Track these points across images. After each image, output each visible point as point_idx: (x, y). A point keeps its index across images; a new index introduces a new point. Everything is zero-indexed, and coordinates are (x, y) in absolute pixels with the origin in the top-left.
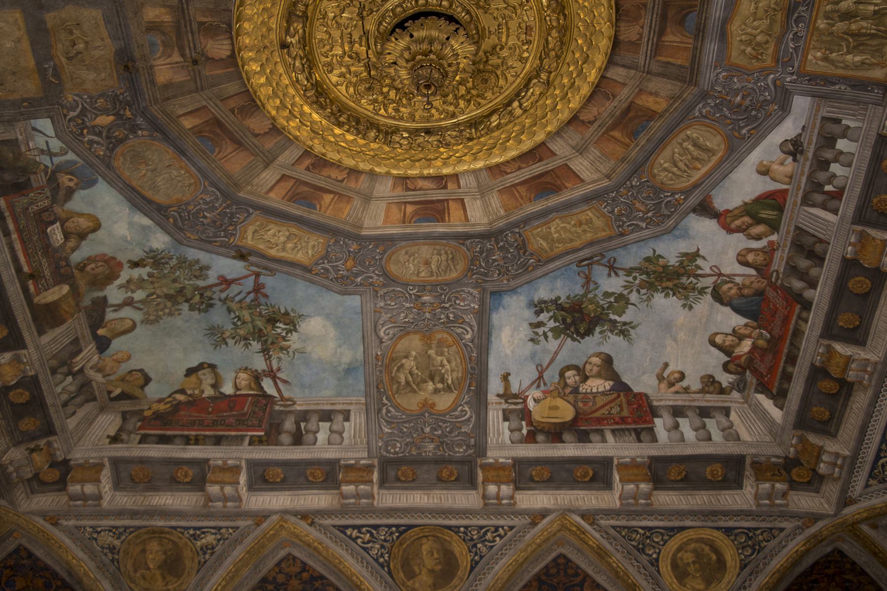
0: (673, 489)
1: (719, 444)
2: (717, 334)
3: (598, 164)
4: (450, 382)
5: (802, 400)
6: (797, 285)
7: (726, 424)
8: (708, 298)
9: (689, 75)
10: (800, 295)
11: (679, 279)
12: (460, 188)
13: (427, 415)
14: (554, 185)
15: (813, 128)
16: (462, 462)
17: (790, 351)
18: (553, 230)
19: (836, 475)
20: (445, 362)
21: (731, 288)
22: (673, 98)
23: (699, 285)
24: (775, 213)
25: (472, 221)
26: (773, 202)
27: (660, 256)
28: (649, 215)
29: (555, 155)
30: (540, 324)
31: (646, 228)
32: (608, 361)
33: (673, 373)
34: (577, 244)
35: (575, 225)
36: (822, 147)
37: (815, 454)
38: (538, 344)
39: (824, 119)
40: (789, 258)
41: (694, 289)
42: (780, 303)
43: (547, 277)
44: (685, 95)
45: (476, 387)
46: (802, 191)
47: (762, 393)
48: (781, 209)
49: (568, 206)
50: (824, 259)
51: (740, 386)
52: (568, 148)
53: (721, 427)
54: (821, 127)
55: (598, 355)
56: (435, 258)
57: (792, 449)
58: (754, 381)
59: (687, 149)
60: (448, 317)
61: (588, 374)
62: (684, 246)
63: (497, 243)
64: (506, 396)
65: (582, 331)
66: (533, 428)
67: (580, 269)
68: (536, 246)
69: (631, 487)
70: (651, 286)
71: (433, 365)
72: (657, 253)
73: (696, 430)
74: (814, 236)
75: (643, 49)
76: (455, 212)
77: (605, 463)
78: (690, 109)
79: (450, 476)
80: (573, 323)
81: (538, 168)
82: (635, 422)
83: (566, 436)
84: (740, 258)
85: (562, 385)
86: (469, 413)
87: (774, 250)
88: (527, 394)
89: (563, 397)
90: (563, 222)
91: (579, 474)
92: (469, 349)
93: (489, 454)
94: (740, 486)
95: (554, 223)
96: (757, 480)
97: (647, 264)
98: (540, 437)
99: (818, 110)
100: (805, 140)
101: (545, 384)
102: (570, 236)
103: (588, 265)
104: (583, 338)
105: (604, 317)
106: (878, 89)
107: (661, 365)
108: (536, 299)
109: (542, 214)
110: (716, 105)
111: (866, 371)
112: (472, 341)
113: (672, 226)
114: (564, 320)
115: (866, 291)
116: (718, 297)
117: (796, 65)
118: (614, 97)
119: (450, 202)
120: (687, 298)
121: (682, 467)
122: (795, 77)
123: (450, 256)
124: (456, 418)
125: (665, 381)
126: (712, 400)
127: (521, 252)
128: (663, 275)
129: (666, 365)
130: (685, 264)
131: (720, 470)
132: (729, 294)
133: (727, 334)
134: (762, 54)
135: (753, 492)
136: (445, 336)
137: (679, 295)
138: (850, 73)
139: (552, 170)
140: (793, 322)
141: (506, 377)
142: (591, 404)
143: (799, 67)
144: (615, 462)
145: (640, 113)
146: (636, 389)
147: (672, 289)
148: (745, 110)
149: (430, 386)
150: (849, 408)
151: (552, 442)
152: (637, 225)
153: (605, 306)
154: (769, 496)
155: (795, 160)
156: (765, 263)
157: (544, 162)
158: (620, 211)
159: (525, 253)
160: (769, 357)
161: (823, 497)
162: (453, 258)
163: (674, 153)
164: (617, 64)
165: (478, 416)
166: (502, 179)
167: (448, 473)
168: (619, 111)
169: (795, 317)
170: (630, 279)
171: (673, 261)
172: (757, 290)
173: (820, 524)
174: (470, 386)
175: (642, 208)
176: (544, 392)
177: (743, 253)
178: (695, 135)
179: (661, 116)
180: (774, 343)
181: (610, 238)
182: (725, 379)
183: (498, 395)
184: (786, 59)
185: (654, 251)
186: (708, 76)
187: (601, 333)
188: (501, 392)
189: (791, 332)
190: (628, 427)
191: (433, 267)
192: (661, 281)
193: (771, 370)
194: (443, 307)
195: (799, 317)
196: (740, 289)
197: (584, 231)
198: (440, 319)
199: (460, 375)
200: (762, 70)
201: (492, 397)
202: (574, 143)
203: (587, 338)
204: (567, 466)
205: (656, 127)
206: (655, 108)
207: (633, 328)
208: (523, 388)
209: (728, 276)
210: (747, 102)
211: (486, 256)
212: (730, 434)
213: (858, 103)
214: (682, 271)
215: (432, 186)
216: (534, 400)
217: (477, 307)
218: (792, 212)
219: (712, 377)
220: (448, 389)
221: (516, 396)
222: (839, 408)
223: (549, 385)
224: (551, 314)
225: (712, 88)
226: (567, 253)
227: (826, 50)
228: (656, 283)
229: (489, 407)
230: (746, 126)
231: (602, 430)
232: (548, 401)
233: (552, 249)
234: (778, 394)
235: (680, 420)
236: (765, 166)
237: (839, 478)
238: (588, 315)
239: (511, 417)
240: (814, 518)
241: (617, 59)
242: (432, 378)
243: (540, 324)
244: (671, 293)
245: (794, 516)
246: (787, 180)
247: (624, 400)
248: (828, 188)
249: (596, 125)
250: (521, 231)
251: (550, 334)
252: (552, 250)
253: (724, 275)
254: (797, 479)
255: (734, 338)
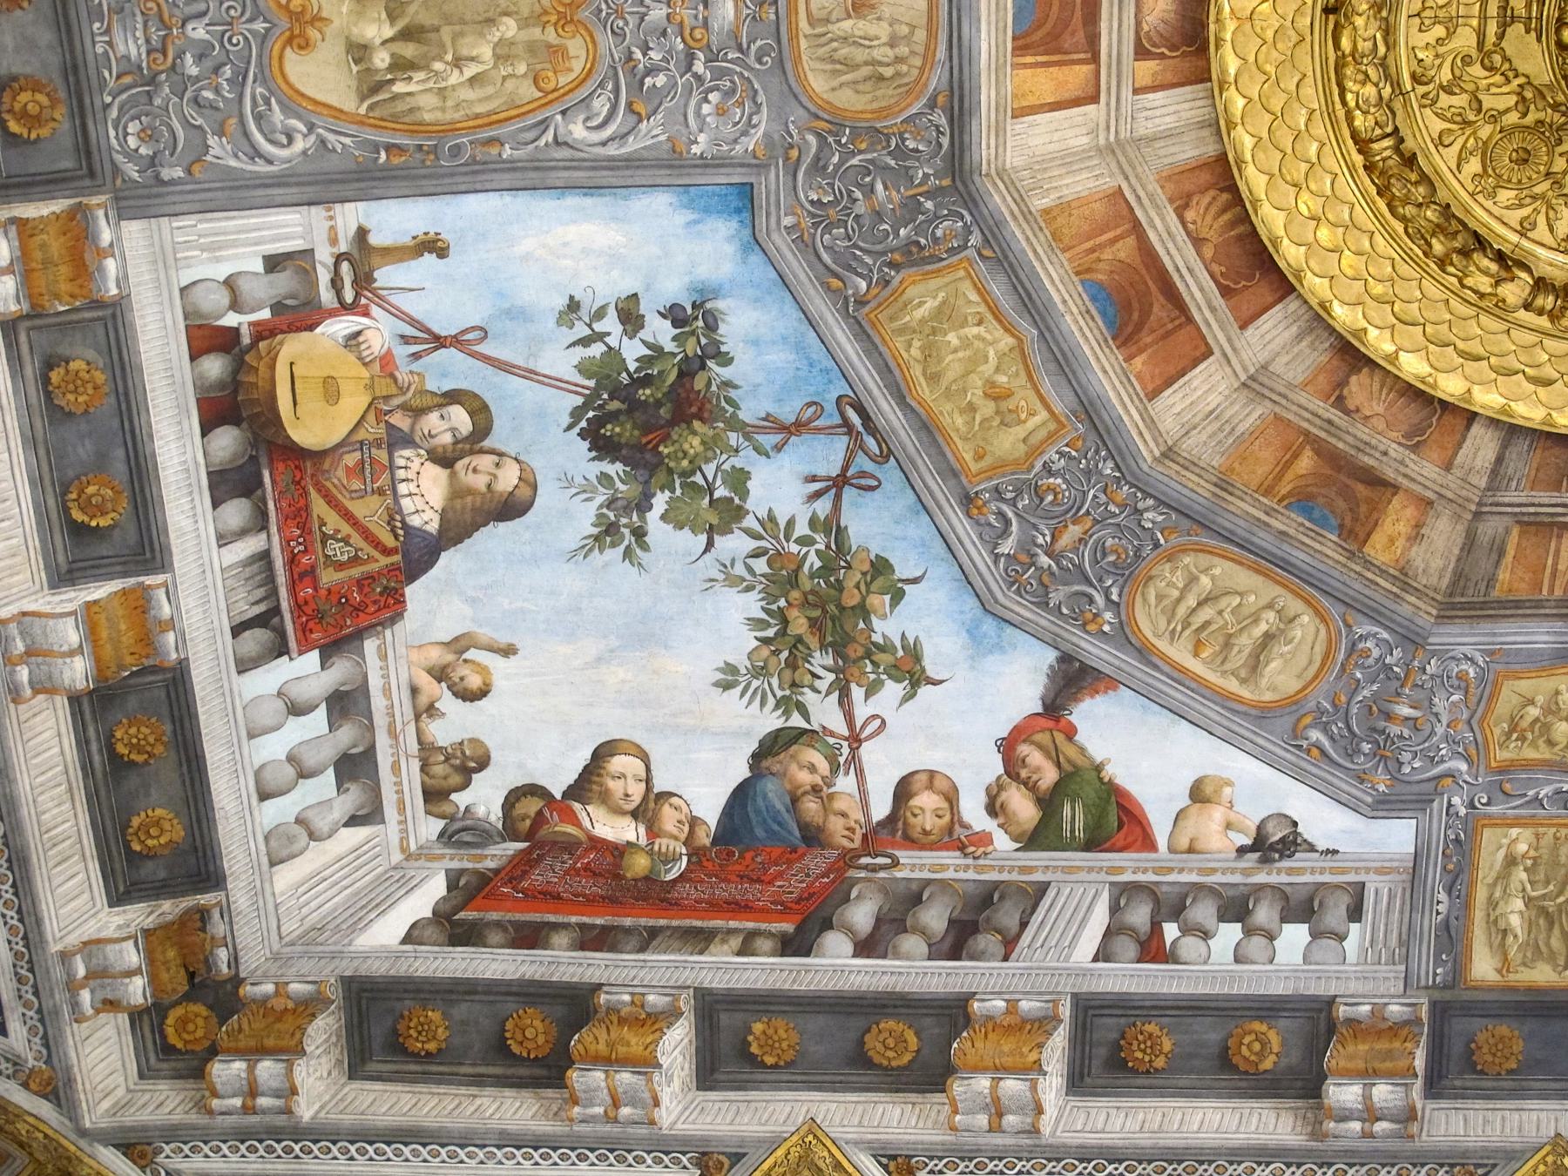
0: (82, 743)
1: (239, 822)
2: (645, 758)
3: (1210, 430)
4: (399, 88)
5: (456, 982)
6: (862, 915)
7: (322, 824)
8: (772, 721)
9: (1467, 599)
10: (827, 925)
11: (823, 647)
12: (1136, 91)
13: (260, 26)
14: (1139, 327)
15: (1333, 871)
16: (85, 148)
17: (628, 931)
18: (975, 330)
19: (215, 1103)
20: (471, 70)
21: (812, 769)
22: (1403, 577)
23: (809, 697)
24: (1080, 834)
25: (1015, 127)
26: (1115, 820)
27: (898, 596)
28: (1044, 560)
29: (1243, 327)
30: (630, 317)
31: (997, 557)
32: (510, 508)
33: (483, 670)
34: (924, 391)
35: (991, 384)
36: (1286, 898)
37: (270, 1042)
38: (559, 323)
39: (1359, 890)
40: (944, 884)
41: (794, 685)
42: (793, 884)
43: (805, 326)
44: (1412, 599)
45: (386, 168)
46: (1150, 877)
47: (452, 885)
48: (1093, 843)
49: (1064, 363)
50: (958, 958)
51: (462, 833)
52: (1263, 357)
53: (310, 814)
54: (1338, 887)
55: (529, 482)
56: (882, 31)
57: (269, 988)
58: (491, 864)
59: (1256, 621)
60: (651, 71)
61: (460, 465)
62: (942, 648)
63: (929, 195)
64: (362, 257)
65: (608, 430)
66: (246, 340)
67: (830, 407)
68: (912, 292)
69: (70, 634)
70: (782, 579)
71: (455, 37)
72: (906, 587)
73: (291, 759)
74: (1024, 925)
75: (1544, 497)
76: (1044, 82)
77: (146, 550)
78: (1373, 614)
79: (23, 116)
80: (634, 406)
81: (1197, 286)
82: (299, 607)
83: (227, 440)
84: (924, 777)
85: (416, 403)
86: (284, 153)
87: (962, 848)
88: (375, 310)
89: (376, 408)
90: (1001, 357)
91: (91, 490)
92: (530, 135)
93: (133, 230)
94: (117, 898)
95: (999, 333)
96: (147, 933)
97: (866, 567)
98: (214, 366)
99: (1380, 871)
100: (1301, 859)
101: (416, 356)
102: (950, 375)
103: (846, 423)
104: (583, 435)
105: (661, 476)
106: (1446, 974)
107: (503, 638)
108: (720, 304)
109: (1031, 303)
110: (1389, 668)
111: (616, 1104)
112: (556, 141)
113: (1008, 615)
114: (647, 381)
115: (877, 1059)
116: (772, 747)
117: (1493, 809)
118: (1415, 448)
119: (1086, 70)
120: (760, 671)
121: (159, 749)
122: (1463, 811)
123: (888, 72)
124: (258, 118)
125: (450, 657)
126: (401, 779)
127: (897, 257)
128: (832, 608)
129: (508, 651)
130: (880, 657)
131: (162, 840)
132: (794, 767)
133: (648, 781)
134: (1523, 739)
135: (110, 932)
136: (578, 66)
137: (765, 652)
138: (1479, 915)
139: (1190, 320)
140: (733, 924)
141: (432, 246)
142: (356, 485)
143: (1490, 817)
144: (149, 580)
145: (1363, 509)
146: (415, 593)
147: (782, 633)
148: (1374, 730)
149: (376, 30)
150: (473, 1090)
151: (198, 400)
152: (1005, 533)
153: (698, 479)
154: (98, 974)
155: (1242, 851)
156: (915, 833)
157: (1219, 301)
158: (1049, 489)
159: (891, 265)
160: (588, 886)
161: (129, 1090)
162: (881, 78)
163: (1241, 594)
164: (1504, 446)
165: (279, 181)
166: (1162, 198)
167: (32, 109)
168: (1371, 462)
169: (750, 925)
170: (802, 529)
171: (887, 627)
172: (820, 829)
173: (44, 1109)
174: (389, 148)
175: (1065, 540)
176: (387, 360)
177: (939, 783)
178: (1298, 633)
179: (1352, 555)
180: (653, 893)
181: (951, 473)
182: (483, 799)
183: (362, 233)
184: (1508, 787)
185: (915, 581)
186: (1465, 642)
187: (604, 478)
188: (374, 240)
189: (698, 923)
190: (283, 592)
191: (847, 25)
192: (806, 603)
193: (550, 897)
194: (690, 58)
195: (751, 936)
196: (816, 790)
197: (972, 408)
198: (646, 49)
199: (427, 117)
200: (1482, 746)
201: (350, 216)
202: (1278, 367)
203: (586, 444)
204: (120, 453)
205: (1327, 549)
206: (1378, 539)
207: (628, 554)
208: (396, 299)
209: (854, 758)
210: (1394, 730)
211: (887, 167)
212: (291, 839)
213: (1405, 943)
214: (855, 651)
215: (1151, 20)
216: (359, 333)
217: (696, 149)
218: (1090, 870)
219: (483, 763)
220: (371, 86)
221: (364, 281)
222: (470, 1070)
223: (416, 367)
224: (670, 347)
225: (1434, 653)
226: (885, 370)
227: (1535, 859)
228: (795, 595)
229: (317, 212)
230: (1332, 739)
231: (263, 526)
232: (349, 370)
233: (901, 331)
234: (453, 924)
235: (321, 713)
236: (1218, 791)
237: (210, 1112)
238: (665, 439)
239: (284, 282)
240: (56, 1086)
241: (1522, 445)
242: (406, 35)
243: (630, 317)
244: (770, 633)
245: (49, 1044)
246: (1184, 843)
247: (374, 567)
248: (1171, 931)
249: (1334, 415)
250: (971, 253)
251: (597, 350)
252: (901, 331)
253: (853, 751)
254: (170, 1021)
255: (637, 799)
